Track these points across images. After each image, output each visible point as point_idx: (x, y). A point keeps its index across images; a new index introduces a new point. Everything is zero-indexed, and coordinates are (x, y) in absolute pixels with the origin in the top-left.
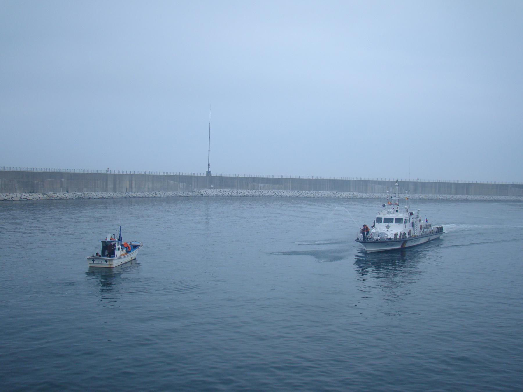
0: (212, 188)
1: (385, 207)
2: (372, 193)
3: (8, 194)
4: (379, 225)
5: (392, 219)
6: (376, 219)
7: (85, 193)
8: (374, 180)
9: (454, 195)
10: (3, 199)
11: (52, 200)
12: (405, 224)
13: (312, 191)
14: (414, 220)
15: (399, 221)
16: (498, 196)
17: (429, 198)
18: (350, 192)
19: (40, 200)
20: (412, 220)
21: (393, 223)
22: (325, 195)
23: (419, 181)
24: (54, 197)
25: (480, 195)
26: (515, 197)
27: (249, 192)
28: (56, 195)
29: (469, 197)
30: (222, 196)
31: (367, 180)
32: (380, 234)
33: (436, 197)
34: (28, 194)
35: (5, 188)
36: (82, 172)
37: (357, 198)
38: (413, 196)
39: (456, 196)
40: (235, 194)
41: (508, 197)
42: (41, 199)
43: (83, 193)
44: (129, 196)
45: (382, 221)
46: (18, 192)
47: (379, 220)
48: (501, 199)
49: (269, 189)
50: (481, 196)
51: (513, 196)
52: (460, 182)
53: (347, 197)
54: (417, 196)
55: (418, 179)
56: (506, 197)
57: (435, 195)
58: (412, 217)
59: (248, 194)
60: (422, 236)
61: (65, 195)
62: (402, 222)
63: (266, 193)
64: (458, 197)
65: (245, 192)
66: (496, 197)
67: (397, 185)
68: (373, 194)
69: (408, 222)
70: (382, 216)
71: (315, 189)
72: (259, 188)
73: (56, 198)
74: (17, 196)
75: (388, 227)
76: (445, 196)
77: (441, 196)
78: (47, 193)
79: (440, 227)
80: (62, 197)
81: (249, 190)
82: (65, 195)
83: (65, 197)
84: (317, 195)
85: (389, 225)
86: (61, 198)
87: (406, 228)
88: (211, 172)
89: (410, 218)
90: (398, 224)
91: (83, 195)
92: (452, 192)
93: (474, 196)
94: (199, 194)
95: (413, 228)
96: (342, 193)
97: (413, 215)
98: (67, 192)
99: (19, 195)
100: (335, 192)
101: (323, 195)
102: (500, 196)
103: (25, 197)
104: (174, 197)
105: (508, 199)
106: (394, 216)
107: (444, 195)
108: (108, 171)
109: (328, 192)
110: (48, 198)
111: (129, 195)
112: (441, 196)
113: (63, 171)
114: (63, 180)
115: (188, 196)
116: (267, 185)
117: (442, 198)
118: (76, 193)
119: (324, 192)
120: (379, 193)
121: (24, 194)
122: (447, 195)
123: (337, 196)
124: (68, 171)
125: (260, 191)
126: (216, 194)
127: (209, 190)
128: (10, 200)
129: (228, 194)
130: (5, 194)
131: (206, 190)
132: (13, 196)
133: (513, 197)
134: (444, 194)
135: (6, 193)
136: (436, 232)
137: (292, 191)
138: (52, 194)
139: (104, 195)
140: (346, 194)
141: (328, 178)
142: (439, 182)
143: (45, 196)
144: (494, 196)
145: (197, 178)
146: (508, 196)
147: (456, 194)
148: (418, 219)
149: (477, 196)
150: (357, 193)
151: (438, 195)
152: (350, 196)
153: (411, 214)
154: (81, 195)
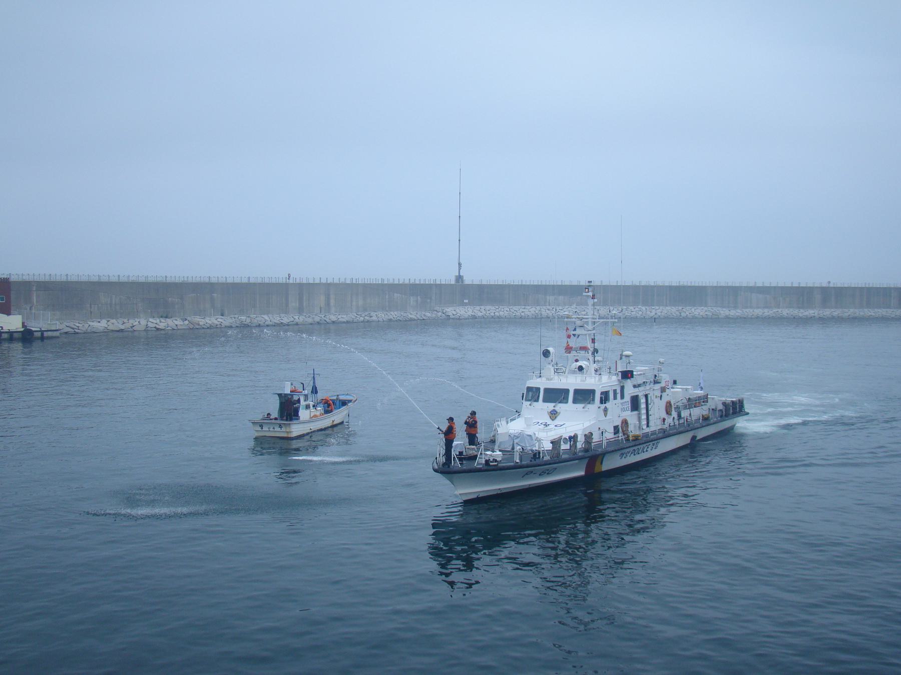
0: (466, 304)
1: (550, 358)
2: (747, 307)
3: (126, 321)
4: (532, 407)
5: (567, 391)
6: (525, 391)
7: (252, 316)
8: (751, 285)
9: (895, 310)
10: (118, 329)
11: (197, 329)
12: (603, 406)
13: (639, 307)
14: (640, 392)
15: (584, 396)
17: (849, 315)
18: (706, 306)
19: (179, 329)
20: (630, 391)
21: (567, 402)
22: (663, 314)
23: (831, 285)
24: (201, 323)
27: (530, 310)
28: (202, 320)
30: (484, 318)
31: (737, 285)
32: (518, 437)
33: (862, 314)
34: (158, 321)
35: (122, 311)
36: (245, 281)
37: (720, 317)
38: (820, 312)
40: (506, 314)
42: (179, 328)
43: (249, 317)
44: (325, 321)
45: (539, 396)
46: (142, 315)
47: (532, 394)
49: (565, 305)
52: (484, 283)
53: (701, 317)
54: (827, 312)
55: (829, 282)
57: (861, 309)
58: (628, 384)
59: (529, 313)
60: (665, 434)
61: (219, 320)
62: (593, 400)
63: (560, 311)
65: (524, 310)
67: (590, 294)
68: (747, 310)
69: (615, 398)
70: (542, 384)
71: (644, 304)
72: (547, 304)
73: (204, 327)
74: (140, 324)
75: (554, 414)
76: (879, 310)
77: (871, 311)
78: (189, 318)
79: (733, 402)
80: (213, 323)
81: (529, 307)
82: (219, 320)
83: (218, 323)
84: (648, 313)
85: (557, 409)
86: (212, 325)
87: (606, 415)
88: (463, 276)
89: (622, 388)
90: (582, 405)
91: (248, 321)
92: (892, 305)
94: (444, 315)
95: (636, 412)
96: (693, 310)
97: (632, 376)
98: (222, 315)
99: (143, 322)
100: (680, 308)
101: (659, 314)
103: (154, 325)
104: (401, 321)
106: (571, 382)
107: (876, 310)
108: (289, 279)
109: (668, 308)
110: (191, 326)
111: (325, 319)
112: (871, 311)
113: (214, 280)
114: (215, 295)
115: (425, 318)
116: (561, 298)
118: (236, 316)
119: (661, 307)
120: (758, 308)
121: (151, 320)
123: (683, 314)
124: (222, 280)
125: (548, 307)
126: (473, 314)
127: (461, 308)
128: (129, 330)
129: (493, 314)
130: (120, 321)
131: (455, 308)
132: (134, 324)
134: (880, 307)
135: (123, 320)
136: (721, 416)
137: (605, 307)
138: (197, 319)
139: (283, 319)
140: (698, 311)
141: (667, 284)
142: (867, 286)
143: (187, 322)
145: (440, 287)
148: (658, 386)
150: (719, 309)
151: (866, 310)
152: (706, 314)
153: (627, 375)
154: (244, 320)
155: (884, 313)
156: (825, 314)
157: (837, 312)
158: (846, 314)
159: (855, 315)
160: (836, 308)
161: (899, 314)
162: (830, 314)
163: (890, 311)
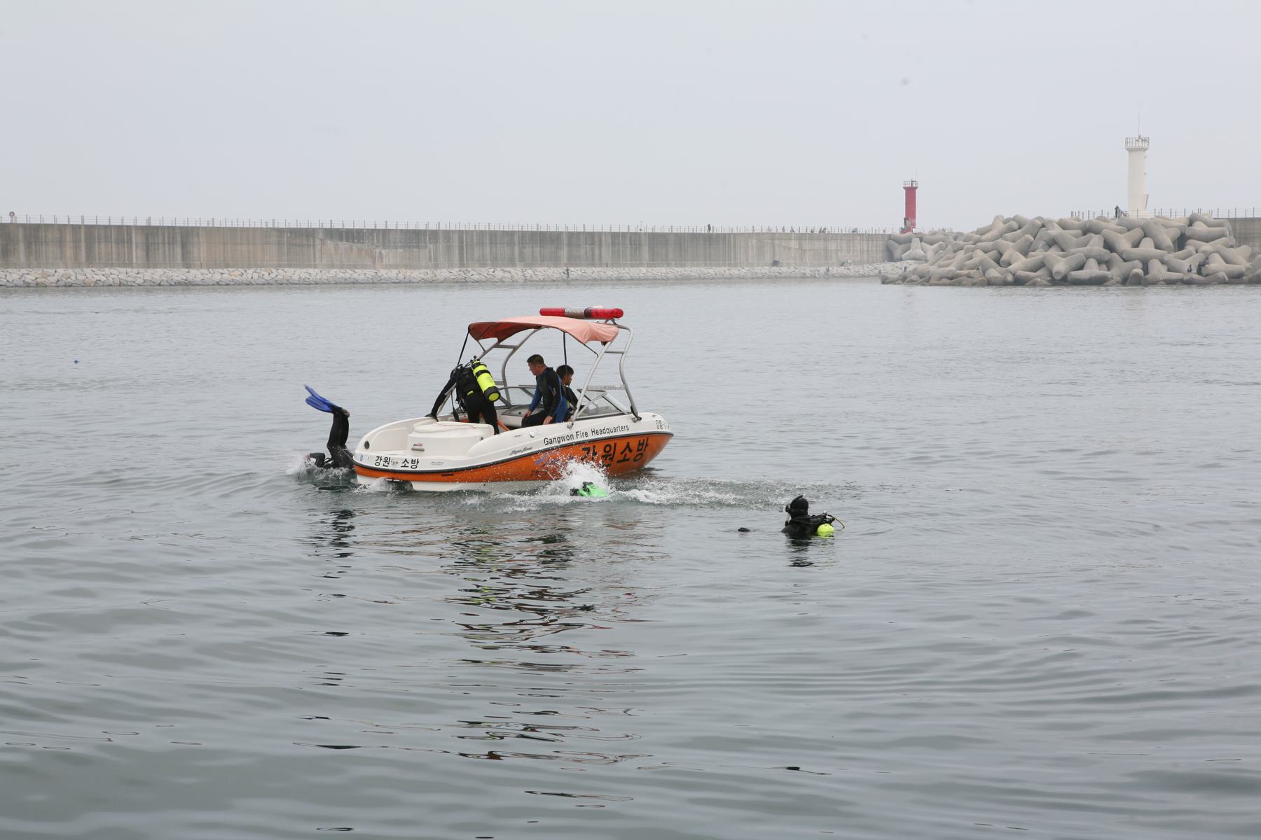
9: (142, 270)
16: (286, 269)
17: (58, 281)
25: (227, 266)
26: (336, 270)
29: (195, 274)
33: (81, 277)
39: (151, 271)
41: (317, 270)
48: (296, 277)
50: (231, 270)
51: (333, 266)
56: (311, 270)
57: (79, 270)
64: (157, 274)
66: (280, 271)
76: (113, 271)
77: (98, 272)
92: (134, 261)
93: (211, 270)
102: (293, 270)
105: (319, 277)
107: (107, 271)
117: (104, 282)
122: (118, 269)
133: (333, 272)
134: (112, 266)
144: (273, 270)
146: (315, 267)
147: (149, 262)
149: (221, 271)
151: (88, 271)
155: (123, 277)
156: (9, 278)
157: (32, 275)
158: (53, 279)
159: (69, 280)
160: (29, 266)
161: (150, 278)
162: (20, 279)
163: (132, 272)
